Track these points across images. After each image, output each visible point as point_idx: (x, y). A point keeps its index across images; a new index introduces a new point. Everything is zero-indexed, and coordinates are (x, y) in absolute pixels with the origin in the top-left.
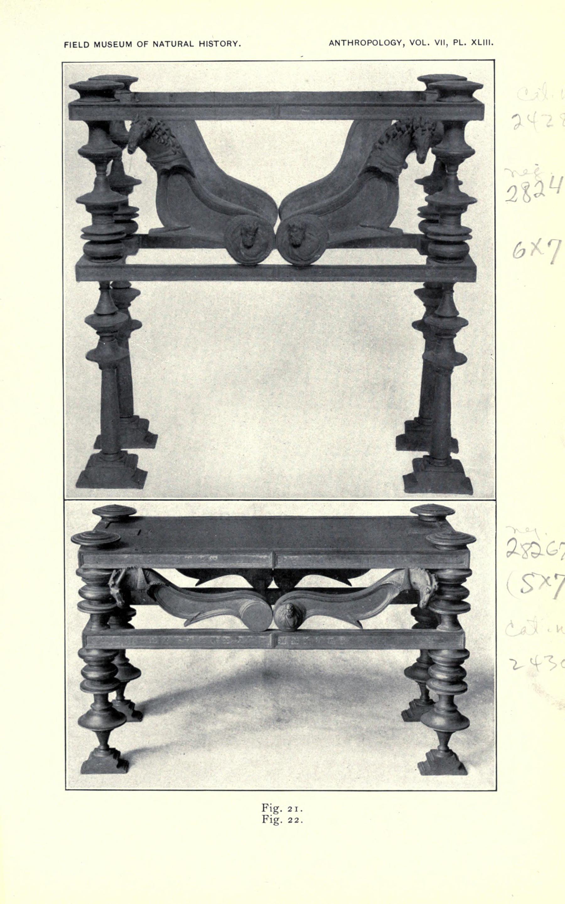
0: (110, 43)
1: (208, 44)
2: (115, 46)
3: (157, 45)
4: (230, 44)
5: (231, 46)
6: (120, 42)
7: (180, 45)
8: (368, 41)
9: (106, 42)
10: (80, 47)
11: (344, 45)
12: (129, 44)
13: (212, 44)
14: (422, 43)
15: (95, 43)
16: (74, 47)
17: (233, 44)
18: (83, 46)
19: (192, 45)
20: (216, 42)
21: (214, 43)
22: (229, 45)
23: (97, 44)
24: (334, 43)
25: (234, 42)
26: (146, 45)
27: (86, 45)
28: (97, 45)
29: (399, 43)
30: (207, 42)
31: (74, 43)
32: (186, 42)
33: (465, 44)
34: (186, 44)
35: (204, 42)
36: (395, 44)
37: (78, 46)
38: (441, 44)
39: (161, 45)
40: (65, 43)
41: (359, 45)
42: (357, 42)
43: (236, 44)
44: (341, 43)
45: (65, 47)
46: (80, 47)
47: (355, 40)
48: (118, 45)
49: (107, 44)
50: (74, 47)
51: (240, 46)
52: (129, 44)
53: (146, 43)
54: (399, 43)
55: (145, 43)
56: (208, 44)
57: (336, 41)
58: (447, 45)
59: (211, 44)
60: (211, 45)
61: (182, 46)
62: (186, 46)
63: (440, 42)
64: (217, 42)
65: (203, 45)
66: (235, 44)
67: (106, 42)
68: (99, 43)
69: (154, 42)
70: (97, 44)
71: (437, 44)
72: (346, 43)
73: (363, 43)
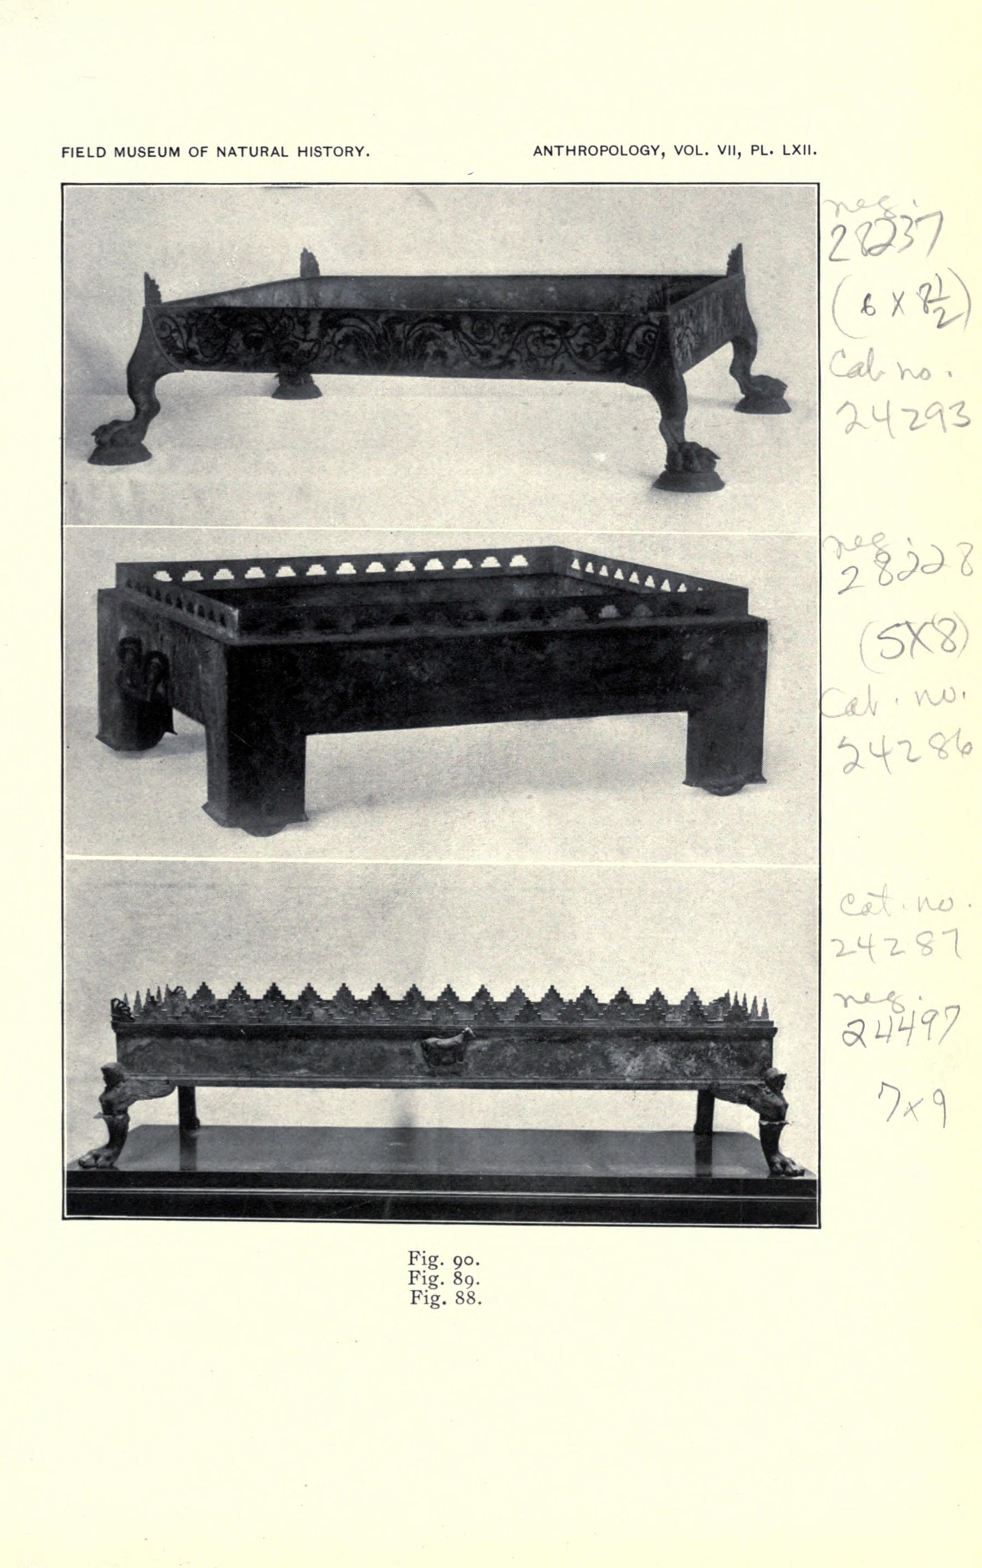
0: (142, 150)
1: (314, 151)
2: (151, 154)
3: (224, 154)
4: (351, 152)
5: (352, 155)
6: (159, 148)
7: (264, 154)
8: (602, 147)
9: (135, 148)
10: (89, 156)
11: (559, 154)
12: (175, 150)
13: (320, 152)
14: (695, 151)
15: (116, 149)
16: (78, 156)
17: (355, 152)
18: (96, 155)
19: (285, 154)
20: (327, 148)
21: (324, 151)
22: (349, 154)
23: (120, 150)
24: (542, 150)
25: (356, 148)
26: (204, 153)
27: (101, 152)
28: (119, 152)
29: (655, 151)
30: (311, 148)
31: (78, 148)
32: (275, 148)
33: (771, 153)
34: (275, 152)
35: (306, 148)
36: (648, 153)
37: (85, 153)
38: (729, 154)
39: (230, 153)
40: (64, 148)
41: (585, 154)
42: (583, 150)
43: (362, 153)
44: (555, 151)
45: (63, 156)
46: (89, 156)
47: (580, 147)
48: (156, 153)
49: (137, 152)
50: (78, 156)
51: (368, 155)
52: (175, 150)
53: (204, 149)
54: (655, 151)
55: (203, 151)
56: (314, 151)
57: (546, 148)
58: (739, 154)
59: (317, 151)
60: (318, 154)
61: (267, 155)
62: (275, 156)
63: (727, 148)
64: (330, 149)
65: (304, 153)
66: (360, 152)
67: (135, 148)
68: (123, 149)
69: (219, 149)
70: (120, 150)
71: (722, 153)
72: (563, 150)
73: (593, 151)
